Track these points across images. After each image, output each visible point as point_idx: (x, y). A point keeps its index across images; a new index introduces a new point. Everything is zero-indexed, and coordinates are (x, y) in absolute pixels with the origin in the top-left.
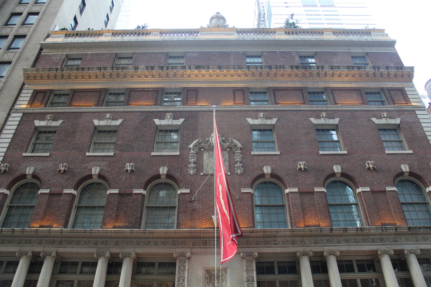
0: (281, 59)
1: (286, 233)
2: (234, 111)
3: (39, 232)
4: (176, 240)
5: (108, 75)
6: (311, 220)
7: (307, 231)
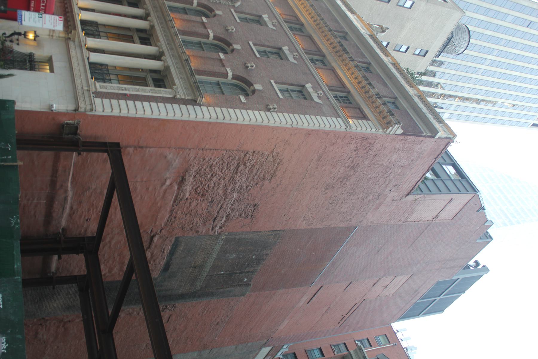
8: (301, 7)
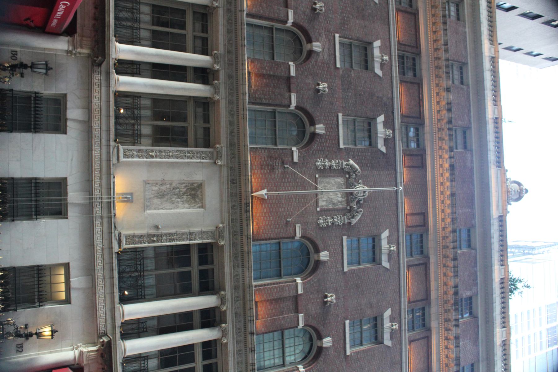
0: (467, 273)
1: (248, 279)
2: (397, 214)
4: (236, 147)
5: (438, 55)
6: (263, 308)
7: (250, 304)
8: (439, 186)
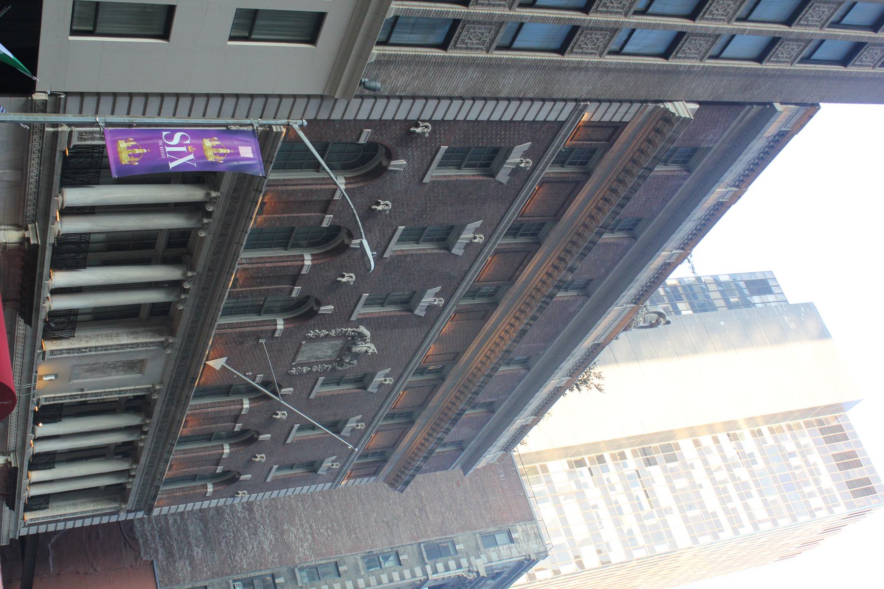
3: (246, 220)
